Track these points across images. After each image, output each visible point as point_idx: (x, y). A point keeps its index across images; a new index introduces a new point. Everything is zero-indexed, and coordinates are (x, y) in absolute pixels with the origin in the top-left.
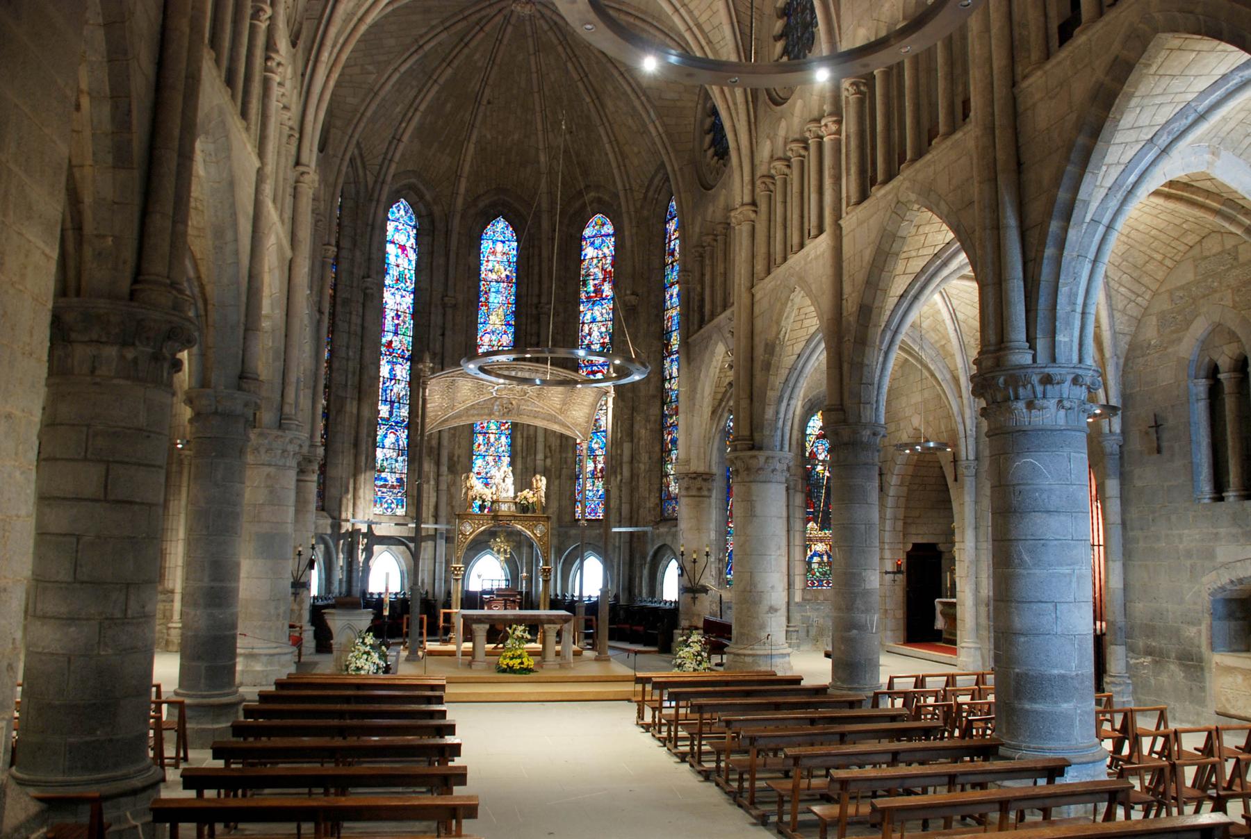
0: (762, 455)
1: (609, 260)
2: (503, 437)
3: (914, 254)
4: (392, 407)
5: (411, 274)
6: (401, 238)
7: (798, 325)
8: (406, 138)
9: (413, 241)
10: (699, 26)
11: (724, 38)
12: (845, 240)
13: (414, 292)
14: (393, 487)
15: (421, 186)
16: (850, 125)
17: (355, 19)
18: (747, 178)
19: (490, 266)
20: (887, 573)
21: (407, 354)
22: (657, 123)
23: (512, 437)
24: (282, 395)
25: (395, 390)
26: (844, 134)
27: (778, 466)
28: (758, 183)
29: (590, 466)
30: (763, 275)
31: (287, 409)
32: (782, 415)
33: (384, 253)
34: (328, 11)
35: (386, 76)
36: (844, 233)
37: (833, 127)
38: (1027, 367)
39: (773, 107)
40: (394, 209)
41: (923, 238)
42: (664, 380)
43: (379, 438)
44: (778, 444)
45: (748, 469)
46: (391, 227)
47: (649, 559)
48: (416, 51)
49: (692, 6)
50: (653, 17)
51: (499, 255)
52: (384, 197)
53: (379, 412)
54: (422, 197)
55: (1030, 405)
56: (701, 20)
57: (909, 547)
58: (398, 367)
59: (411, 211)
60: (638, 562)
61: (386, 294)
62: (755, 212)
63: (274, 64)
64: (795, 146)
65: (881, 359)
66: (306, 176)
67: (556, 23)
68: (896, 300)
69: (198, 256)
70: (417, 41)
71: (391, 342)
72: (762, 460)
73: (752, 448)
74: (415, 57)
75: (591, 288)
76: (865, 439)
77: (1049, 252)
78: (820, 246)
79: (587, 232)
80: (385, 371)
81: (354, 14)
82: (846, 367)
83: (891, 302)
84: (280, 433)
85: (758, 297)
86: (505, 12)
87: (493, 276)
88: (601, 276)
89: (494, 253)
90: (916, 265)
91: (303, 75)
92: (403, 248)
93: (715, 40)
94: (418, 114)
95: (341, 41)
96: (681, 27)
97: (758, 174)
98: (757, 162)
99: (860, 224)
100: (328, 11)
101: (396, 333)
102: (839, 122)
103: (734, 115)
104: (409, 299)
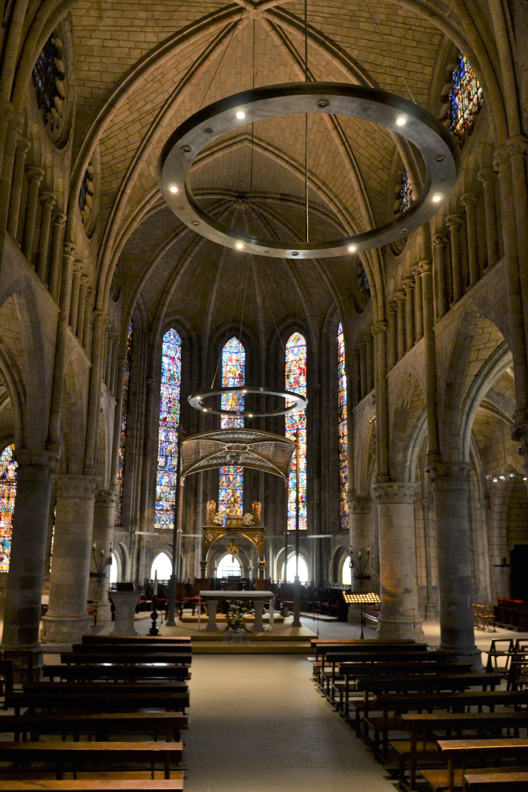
0: (396, 486)
1: (303, 362)
2: (238, 476)
3: (482, 346)
4: (166, 460)
5: (178, 375)
6: (172, 354)
7: (416, 398)
8: (172, 291)
9: (179, 354)
10: (346, 209)
11: (362, 216)
12: (437, 341)
13: (181, 386)
14: (167, 510)
15: (183, 320)
16: (437, 265)
17: (130, 219)
18: (380, 304)
19: (229, 368)
20: (496, 566)
21: (176, 426)
22: (328, 272)
23: (244, 476)
24: (85, 454)
25: (168, 449)
26: (433, 271)
27: (407, 492)
28: (388, 306)
30: (392, 366)
31: (88, 462)
32: (409, 458)
33: (161, 362)
34: (112, 215)
35: (157, 252)
36: (436, 336)
37: (426, 267)
39: (395, 257)
40: (167, 335)
41: (488, 336)
42: (339, 437)
43: (158, 479)
44: (407, 477)
45: (387, 495)
46: (164, 347)
47: (332, 556)
48: (175, 237)
49: (341, 197)
50: (320, 205)
51: (234, 363)
52: (160, 328)
54: (184, 327)
56: (348, 205)
57: (512, 548)
58: (170, 434)
59: (177, 336)
60: (325, 558)
61: (162, 389)
62: (387, 326)
63: (69, 249)
64: (407, 281)
65: (464, 418)
66: (100, 317)
67: (262, 214)
68: (473, 378)
69: (21, 367)
70: (174, 230)
71: (166, 418)
72: (396, 488)
73: (390, 480)
74: (175, 241)
75: (292, 380)
76: (455, 472)
78: (421, 345)
79: (289, 344)
80: (162, 436)
81: (128, 216)
82: (440, 424)
83: (469, 380)
84: (83, 477)
85: (390, 381)
86: (230, 209)
87: (231, 375)
88: (298, 372)
89: (231, 360)
90: (485, 354)
91: (98, 255)
92: (173, 359)
93: (357, 217)
94: (179, 277)
95: (121, 233)
96: (335, 210)
97: (388, 300)
98: (386, 293)
99: (444, 328)
100: (112, 215)
101: (169, 413)
102: (430, 263)
103: (371, 264)
104: (177, 391)
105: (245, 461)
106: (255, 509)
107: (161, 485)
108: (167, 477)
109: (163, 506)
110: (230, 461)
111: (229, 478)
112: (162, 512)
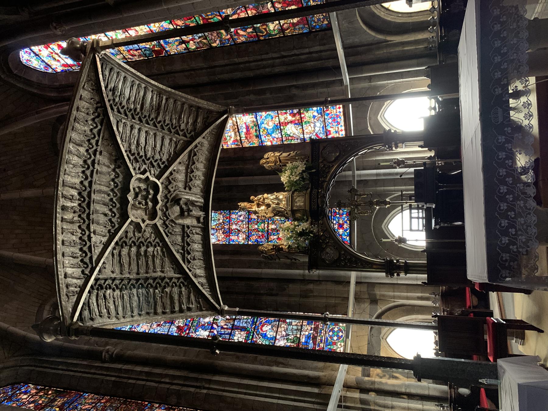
4: (238, 328)
29: (291, 129)
47: (380, 37)
53: (240, 342)
105: (197, 190)
106: (275, 162)
107: (275, 338)
108: (265, 328)
109: (308, 337)
110: (198, 219)
111: (273, 230)
112: (319, 338)
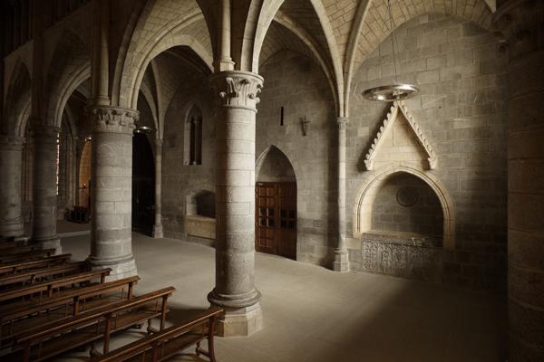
38: (107, 106)
55: (107, 123)
77: (119, 60)
